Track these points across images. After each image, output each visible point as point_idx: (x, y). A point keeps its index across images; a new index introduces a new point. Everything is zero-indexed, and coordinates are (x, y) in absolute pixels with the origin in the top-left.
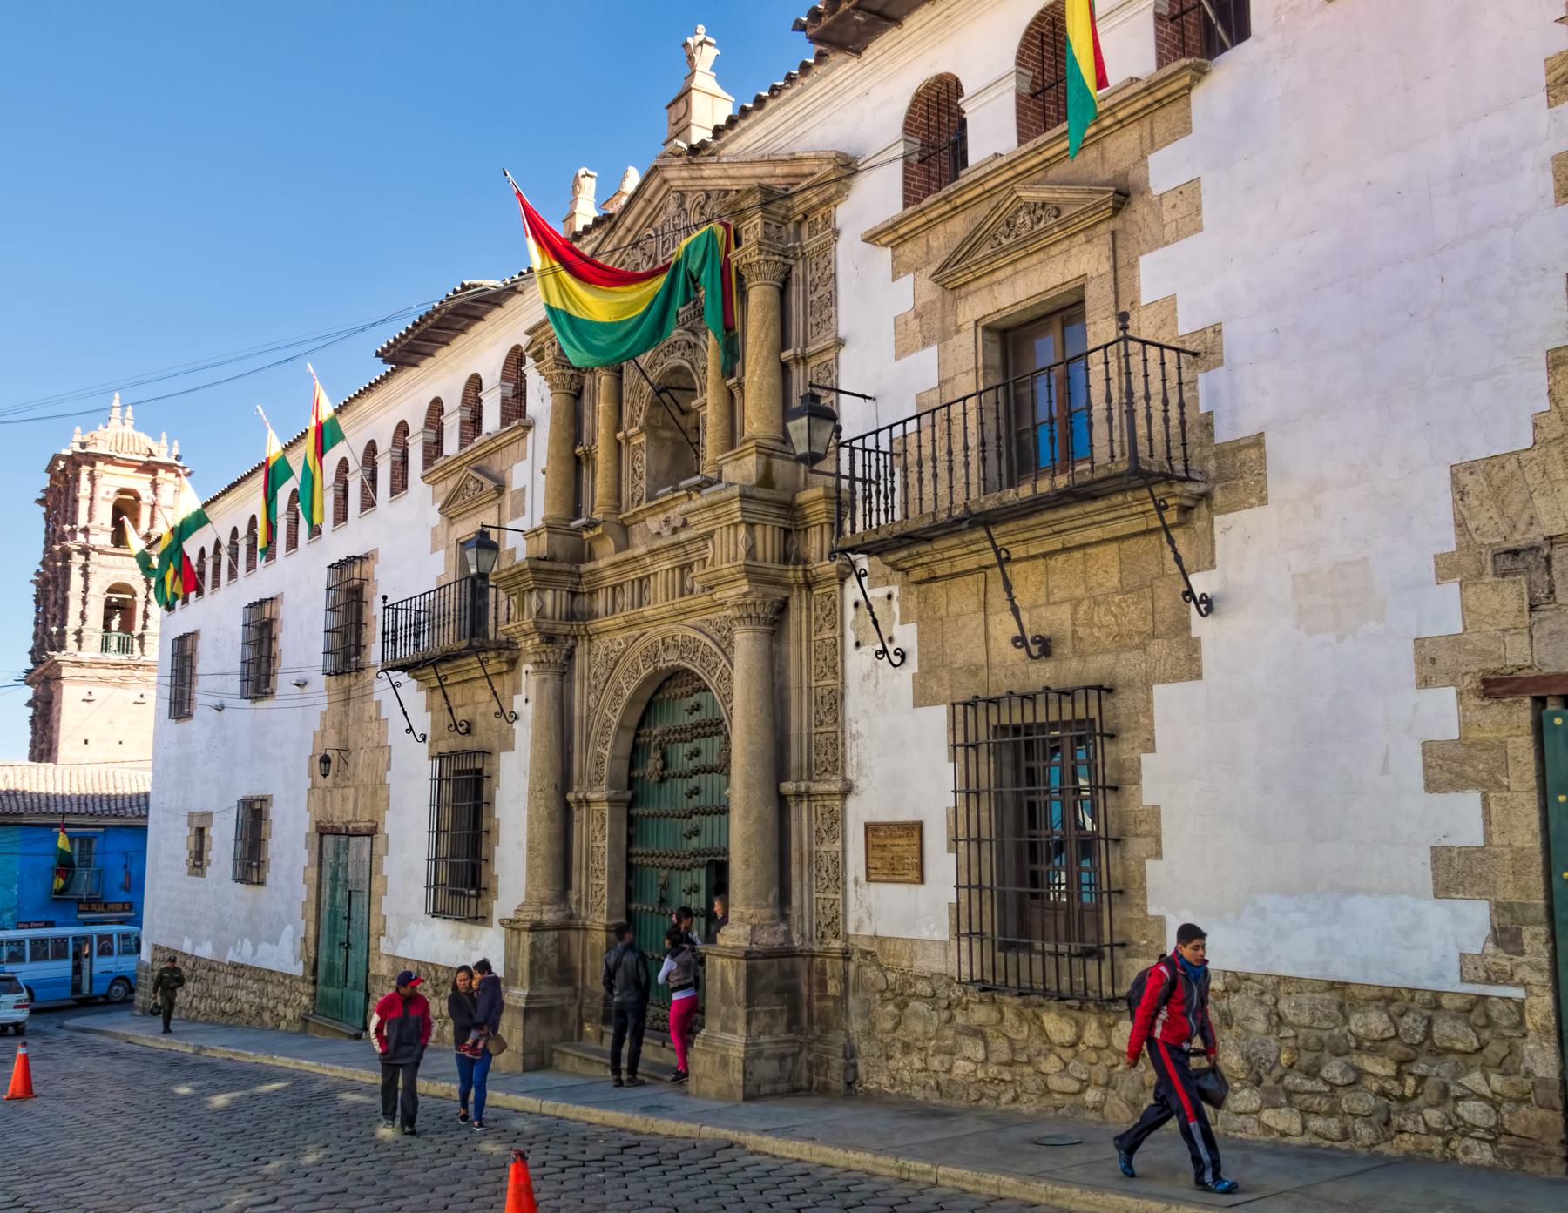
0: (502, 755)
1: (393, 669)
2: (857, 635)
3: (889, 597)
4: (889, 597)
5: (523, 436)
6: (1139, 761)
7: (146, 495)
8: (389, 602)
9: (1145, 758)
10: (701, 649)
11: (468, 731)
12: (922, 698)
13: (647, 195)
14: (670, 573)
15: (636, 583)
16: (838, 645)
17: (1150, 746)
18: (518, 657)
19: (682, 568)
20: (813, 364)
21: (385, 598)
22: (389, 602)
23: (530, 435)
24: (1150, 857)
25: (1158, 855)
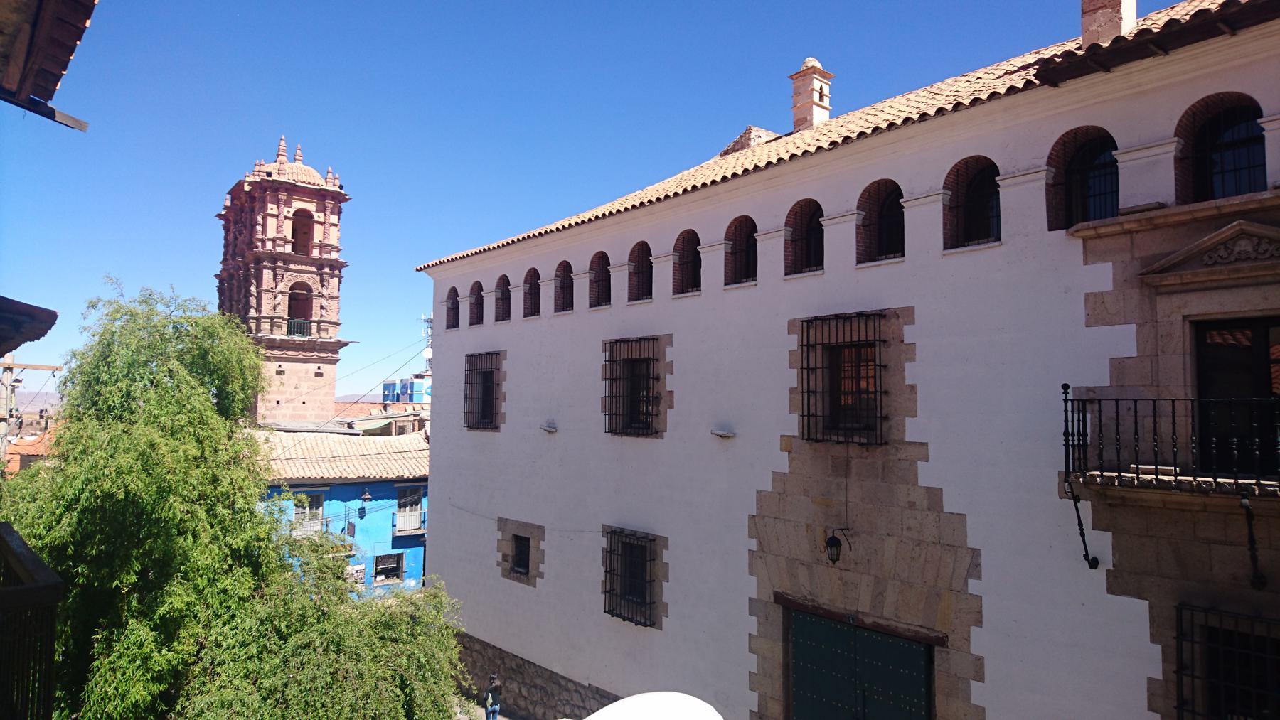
7: (319, 217)
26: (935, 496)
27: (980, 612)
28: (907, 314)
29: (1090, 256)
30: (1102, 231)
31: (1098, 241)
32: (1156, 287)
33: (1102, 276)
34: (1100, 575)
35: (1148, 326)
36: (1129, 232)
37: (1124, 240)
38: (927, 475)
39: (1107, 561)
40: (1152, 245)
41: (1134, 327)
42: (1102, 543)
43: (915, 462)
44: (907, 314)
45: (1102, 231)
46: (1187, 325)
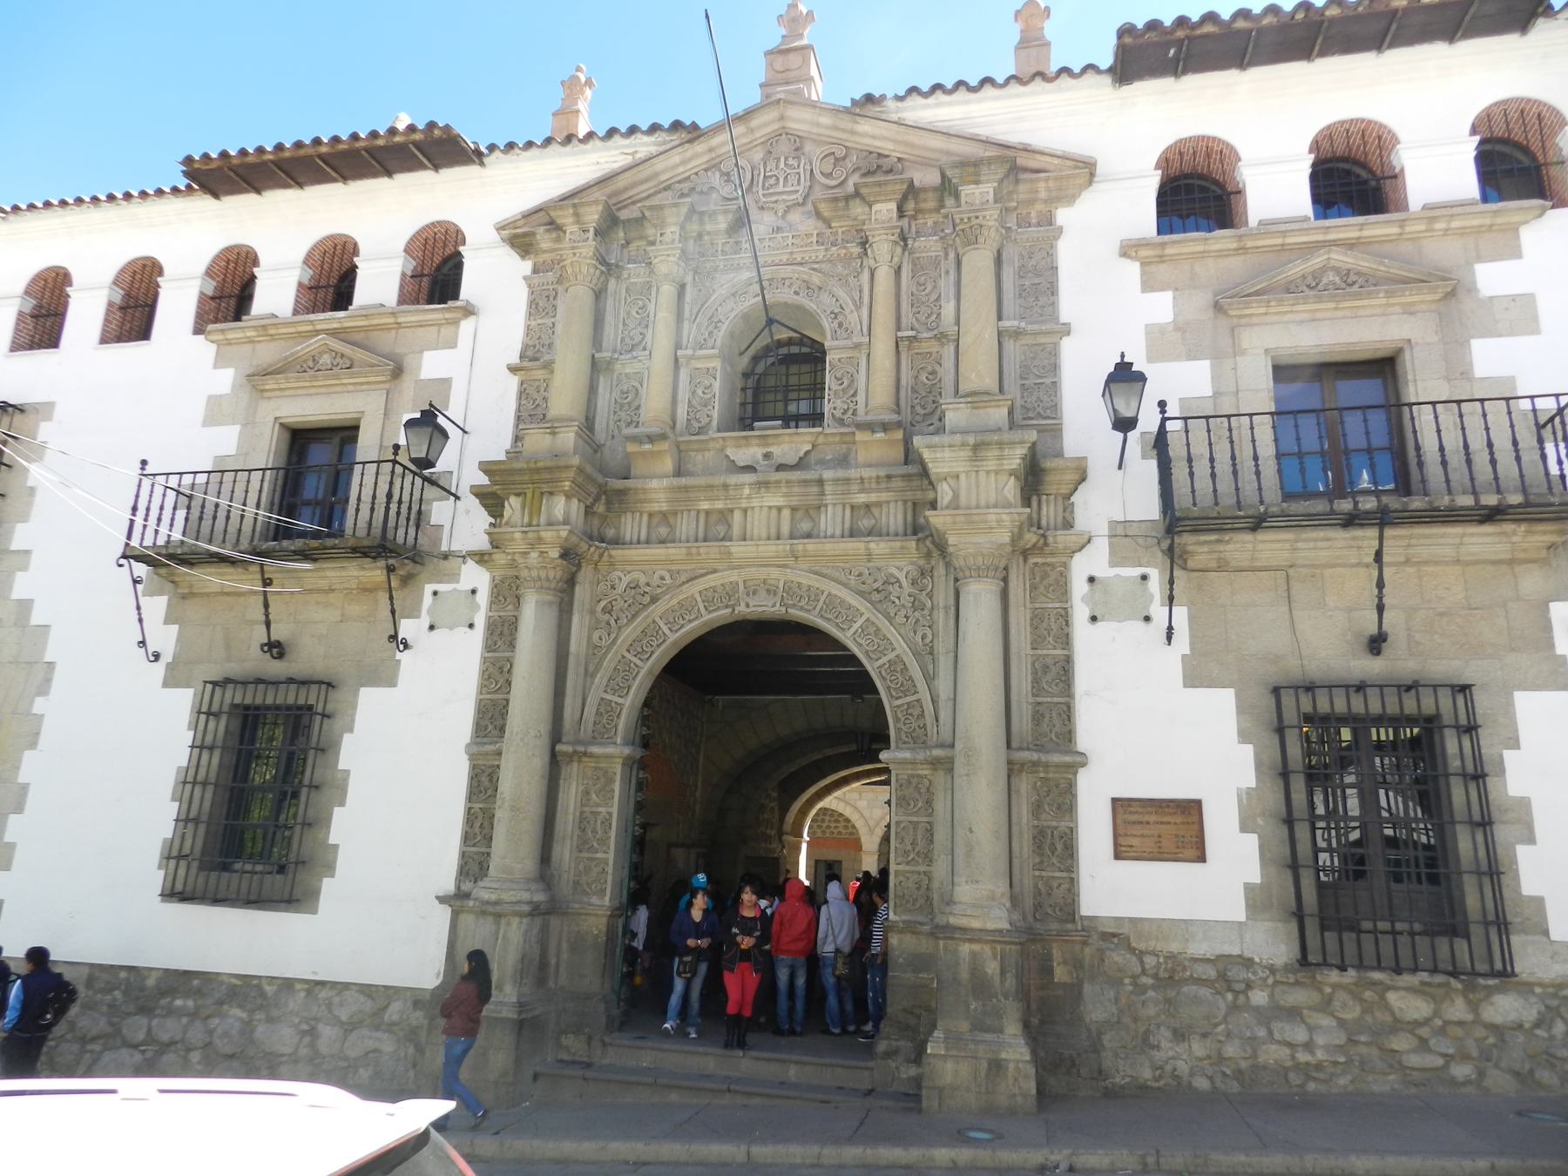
0: (363, 691)
1: (140, 558)
2: (1092, 610)
3: (1144, 577)
4: (1144, 577)
5: (455, 323)
6: (1501, 757)
8: (149, 470)
9: (1508, 755)
10: (823, 599)
11: (281, 656)
12: (1195, 676)
13: (754, 123)
14: (774, 512)
15: (702, 517)
16: (1065, 618)
17: (1515, 743)
18: (419, 574)
19: (794, 509)
20: (1024, 342)
21: (144, 463)
22: (149, 470)
23: (466, 326)
24: (1523, 842)
25: (1531, 840)
26: (25, 606)
27: (38, 734)
28: (44, 410)
29: (219, 362)
30: (230, 336)
31: (229, 348)
32: (262, 391)
33: (224, 380)
34: (159, 669)
35: (248, 423)
36: (251, 341)
37: (248, 347)
38: (22, 587)
39: (167, 657)
40: (268, 353)
41: (237, 428)
42: (165, 638)
43: (13, 572)
44: (44, 410)
45: (230, 336)
46: (277, 426)
